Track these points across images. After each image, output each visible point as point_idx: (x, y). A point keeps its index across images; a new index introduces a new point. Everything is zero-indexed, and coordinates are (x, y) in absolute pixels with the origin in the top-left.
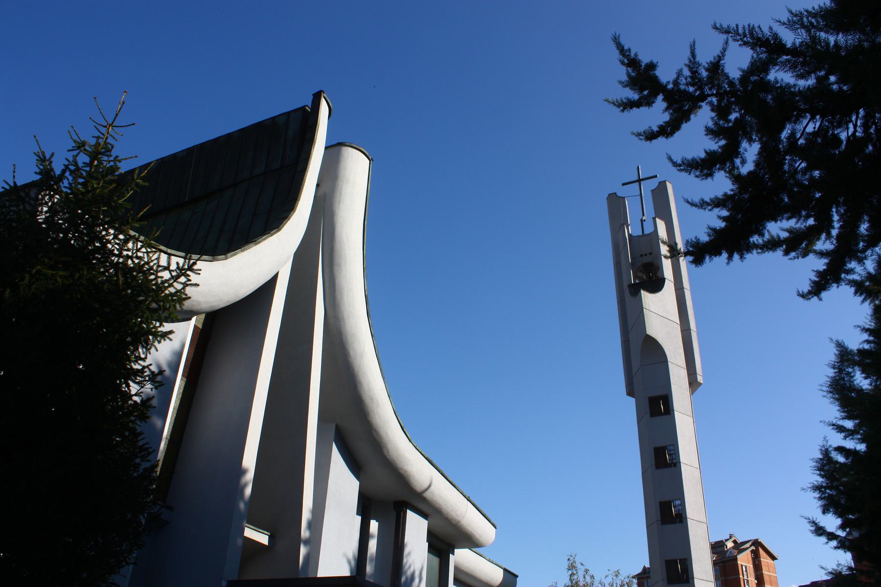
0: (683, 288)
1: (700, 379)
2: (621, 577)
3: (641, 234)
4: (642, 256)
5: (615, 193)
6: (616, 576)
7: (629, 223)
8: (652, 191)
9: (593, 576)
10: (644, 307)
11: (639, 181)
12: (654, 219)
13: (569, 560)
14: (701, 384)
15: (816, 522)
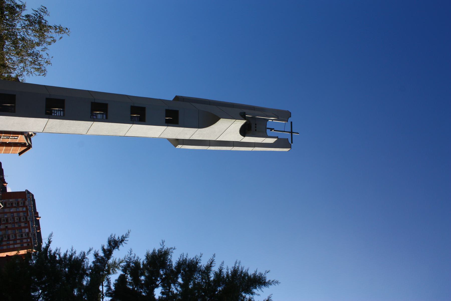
0: (234, 146)
1: (179, 146)
2: (45, 65)
3: (267, 127)
4: (256, 125)
5: (291, 117)
6: (47, 62)
7: (273, 121)
8: (288, 139)
9: (50, 44)
10: (237, 120)
11: (292, 132)
12: (277, 137)
13: (67, 29)
14: (176, 146)
15: (123, 243)
